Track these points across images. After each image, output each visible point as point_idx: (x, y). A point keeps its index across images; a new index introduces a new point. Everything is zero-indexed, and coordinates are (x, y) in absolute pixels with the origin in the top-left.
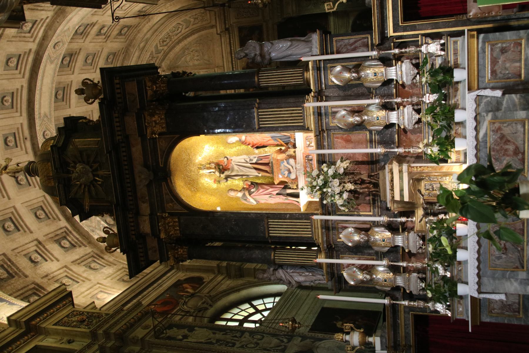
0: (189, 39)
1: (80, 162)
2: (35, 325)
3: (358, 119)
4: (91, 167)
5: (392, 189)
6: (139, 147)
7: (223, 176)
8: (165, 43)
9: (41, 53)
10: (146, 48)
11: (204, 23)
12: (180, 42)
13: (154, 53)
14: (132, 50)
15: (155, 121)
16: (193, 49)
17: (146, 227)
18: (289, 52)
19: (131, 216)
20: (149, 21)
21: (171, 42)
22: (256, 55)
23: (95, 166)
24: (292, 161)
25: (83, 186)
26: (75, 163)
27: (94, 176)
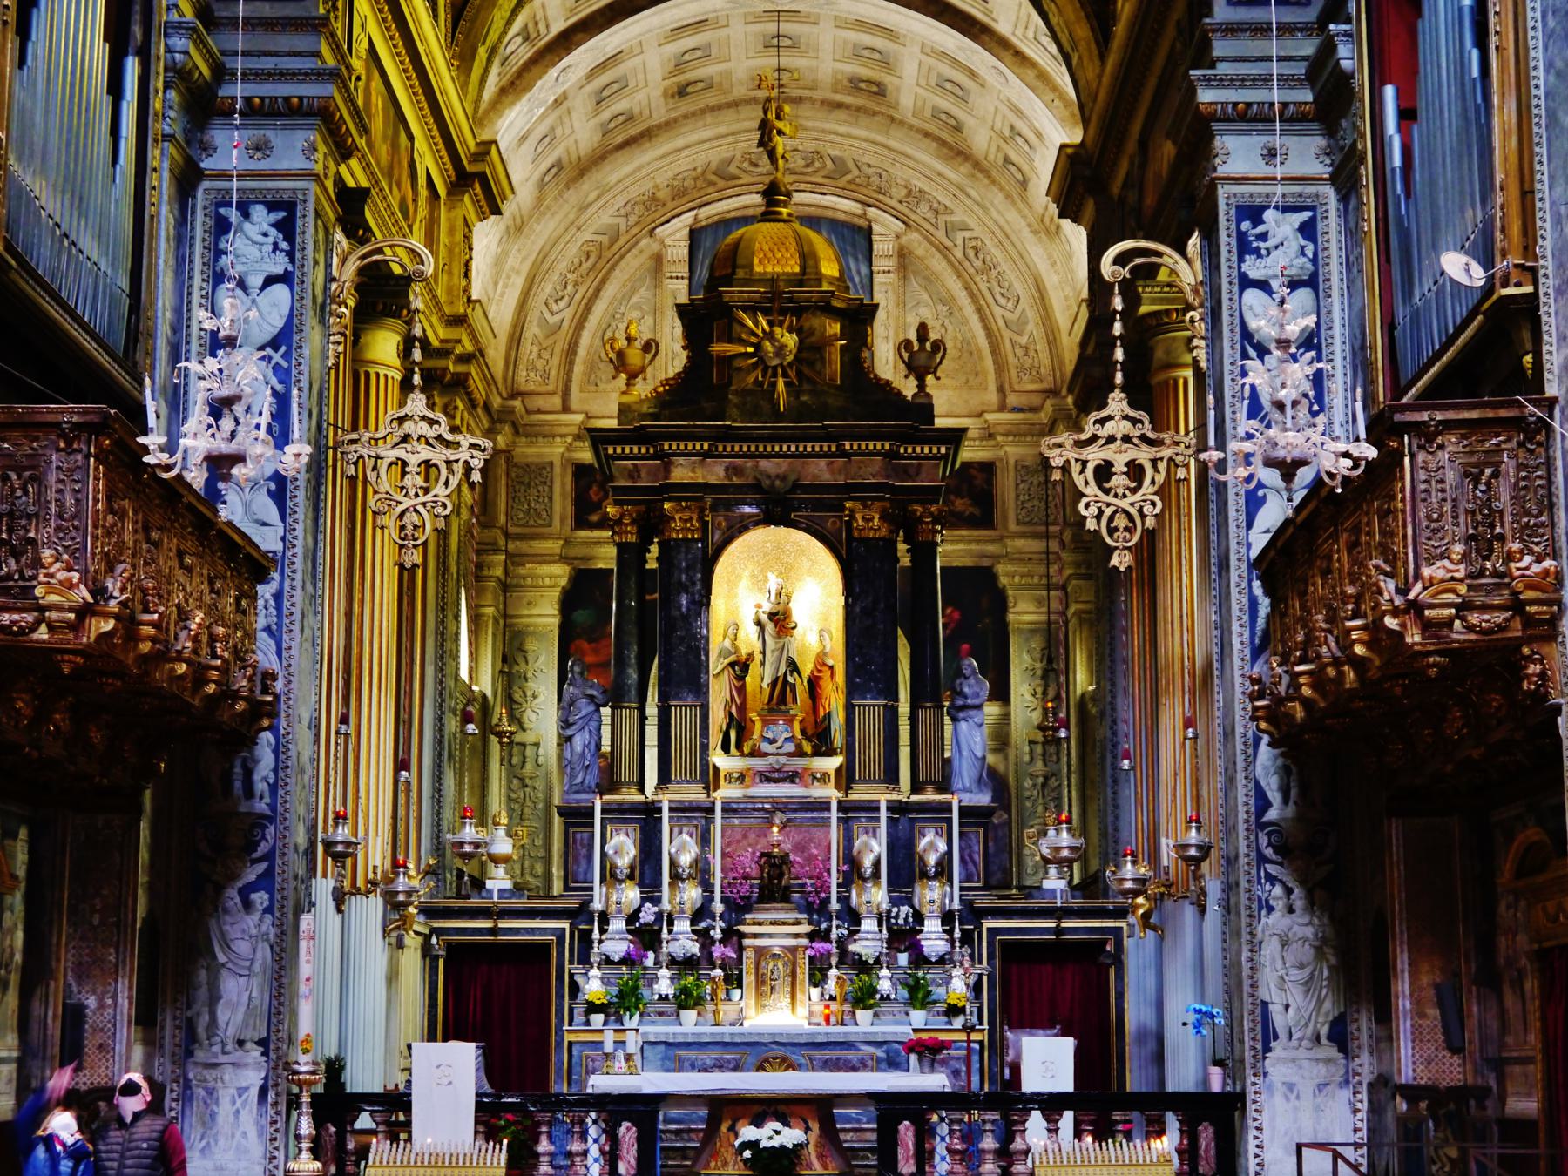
0: (974, 320)
1: (801, 341)
2: (472, 186)
3: (869, 872)
4: (790, 364)
5: (773, 923)
6: (827, 478)
7: (764, 618)
8: (971, 253)
9: (985, 38)
10: (963, 197)
11: (1013, 373)
12: (971, 295)
13: (948, 218)
14: (962, 169)
15: (872, 520)
16: (950, 327)
17: (681, 473)
18: (965, 753)
19: (706, 447)
20: (1035, 232)
21: (972, 271)
22: (966, 697)
23: (792, 373)
24: (790, 747)
25: (753, 340)
26: (799, 331)
27: (775, 368)
